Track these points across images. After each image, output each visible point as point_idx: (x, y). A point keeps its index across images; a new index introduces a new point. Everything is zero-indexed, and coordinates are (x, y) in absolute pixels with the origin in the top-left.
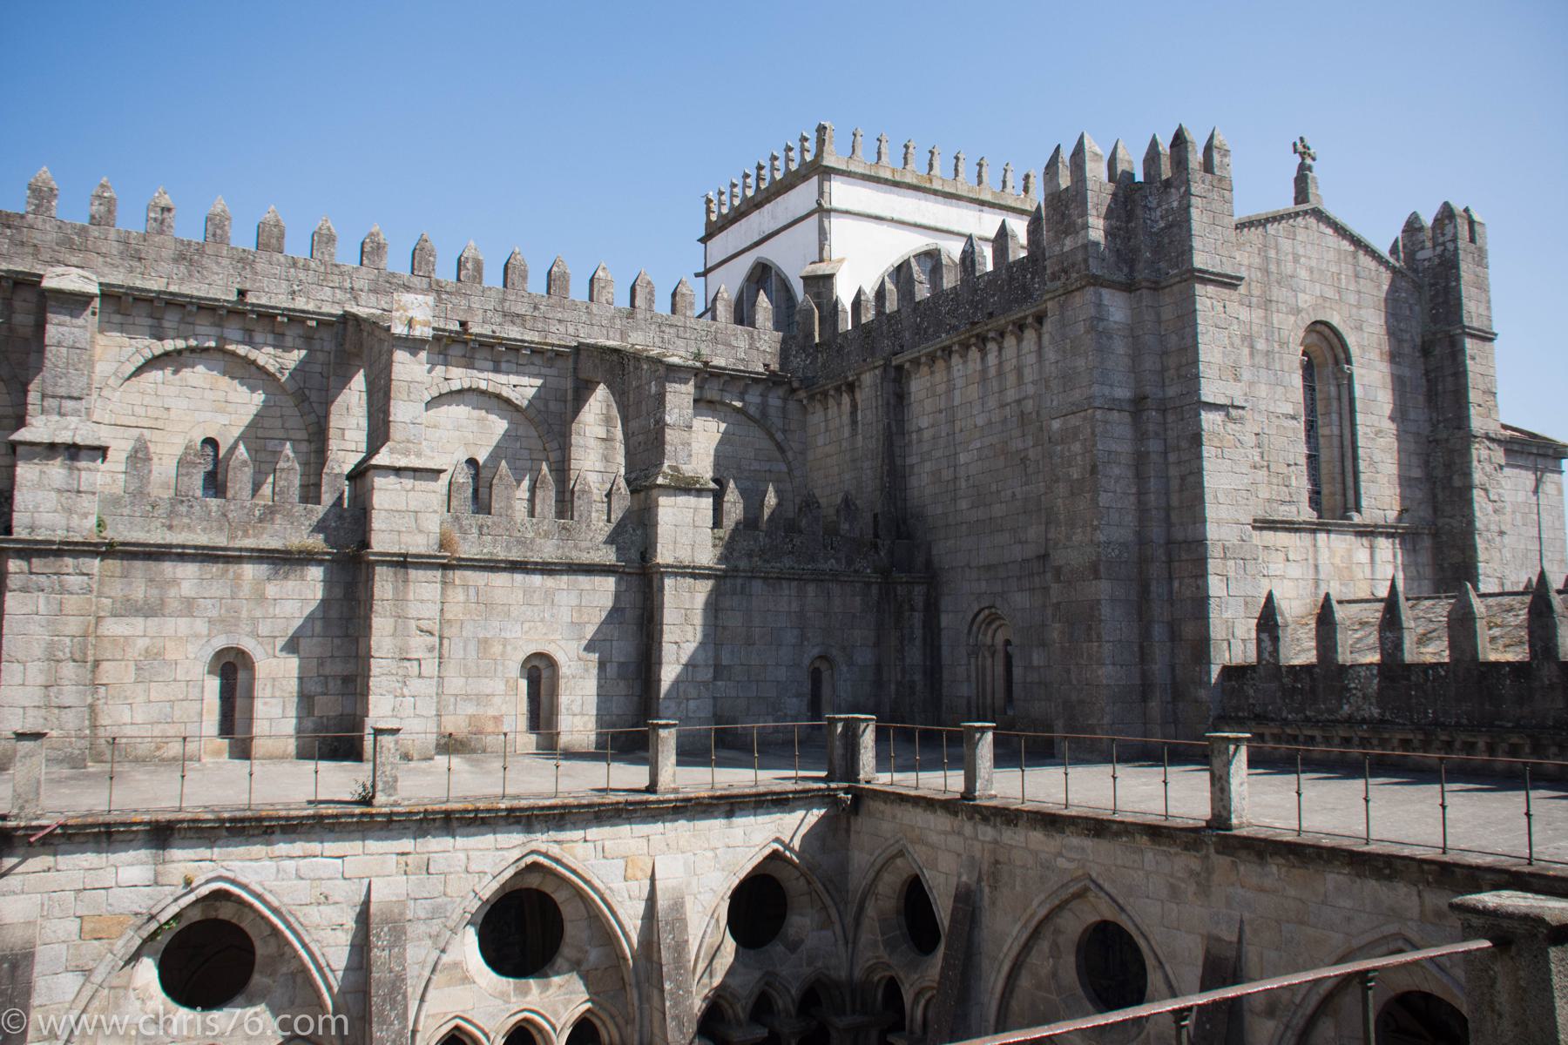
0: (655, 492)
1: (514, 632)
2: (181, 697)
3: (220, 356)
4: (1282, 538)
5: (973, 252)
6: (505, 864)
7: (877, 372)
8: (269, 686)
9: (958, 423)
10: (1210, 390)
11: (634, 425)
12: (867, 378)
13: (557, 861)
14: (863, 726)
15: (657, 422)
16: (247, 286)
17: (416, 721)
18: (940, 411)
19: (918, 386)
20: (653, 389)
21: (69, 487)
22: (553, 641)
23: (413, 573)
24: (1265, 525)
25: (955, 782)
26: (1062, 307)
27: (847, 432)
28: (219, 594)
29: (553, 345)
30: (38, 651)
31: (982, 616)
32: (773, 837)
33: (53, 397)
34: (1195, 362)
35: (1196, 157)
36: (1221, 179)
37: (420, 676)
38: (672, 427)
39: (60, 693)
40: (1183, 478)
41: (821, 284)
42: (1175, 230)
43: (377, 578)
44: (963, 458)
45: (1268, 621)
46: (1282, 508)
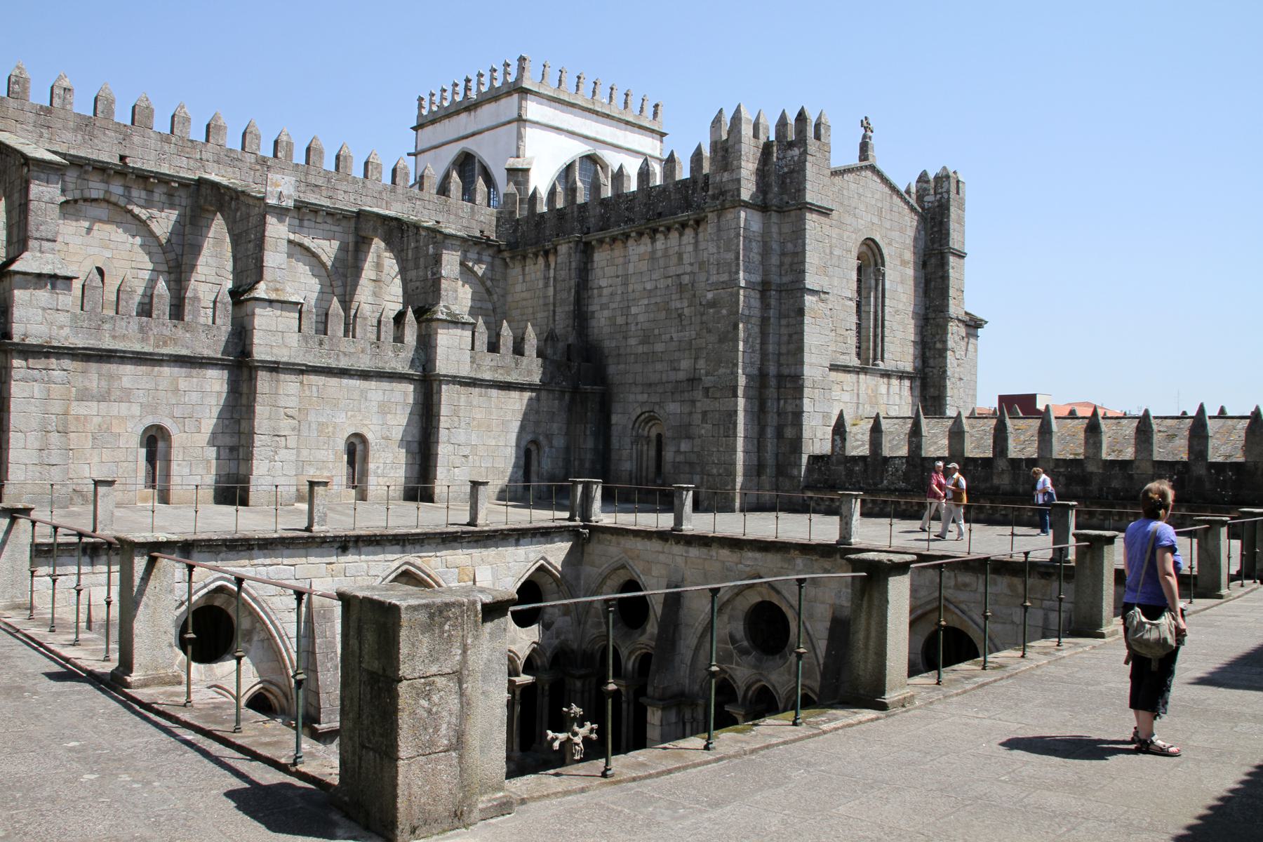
0: (434, 324)
1: (341, 418)
2: (123, 459)
3: (105, 205)
4: (841, 376)
5: (648, 170)
6: (390, 570)
7: (571, 245)
8: (181, 453)
9: (630, 288)
10: (811, 281)
11: (412, 274)
12: (563, 249)
13: (419, 568)
14: (595, 486)
15: (433, 274)
16: (127, 153)
17: (283, 478)
18: (618, 277)
19: (600, 257)
20: (431, 250)
21: (50, 306)
22: (366, 425)
23: (282, 376)
24: (834, 368)
25: (665, 521)
26: (719, 217)
27: (541, 284)
28: (148, 386)
29: (342, 210)
30: (34, 424)
31: (643, 417)
32: (540, 556)
33: (36, 239)
34: (803, 262)
35: (810, 132)
36: (824, 144)
37: (286, 448)
38: (446, 278)
39: (49, 455)
40: (790, 336)
41: (518, 175)
42: (795, 175)
43: (259, 378)
44: (634, 310)
45: (839, 430)
46: (842, 357)
